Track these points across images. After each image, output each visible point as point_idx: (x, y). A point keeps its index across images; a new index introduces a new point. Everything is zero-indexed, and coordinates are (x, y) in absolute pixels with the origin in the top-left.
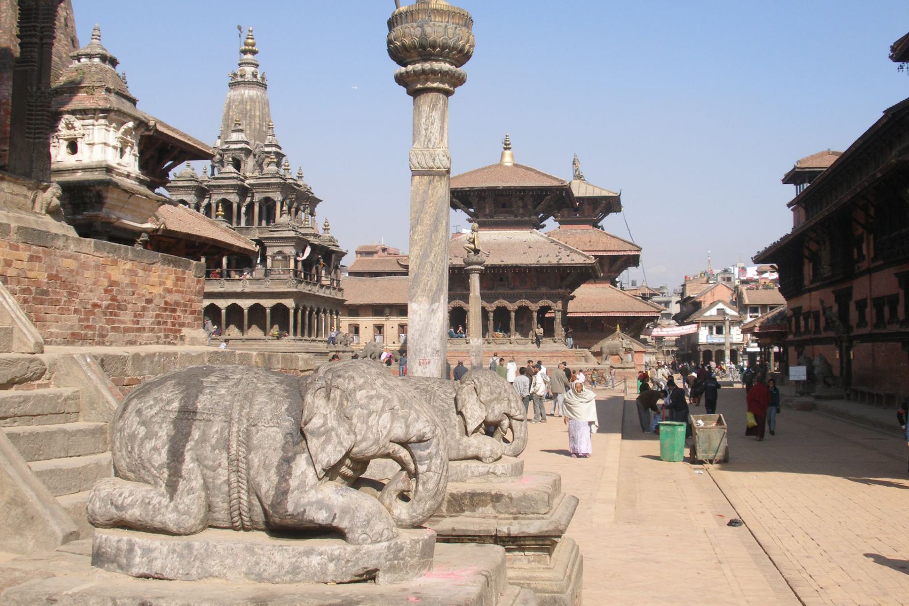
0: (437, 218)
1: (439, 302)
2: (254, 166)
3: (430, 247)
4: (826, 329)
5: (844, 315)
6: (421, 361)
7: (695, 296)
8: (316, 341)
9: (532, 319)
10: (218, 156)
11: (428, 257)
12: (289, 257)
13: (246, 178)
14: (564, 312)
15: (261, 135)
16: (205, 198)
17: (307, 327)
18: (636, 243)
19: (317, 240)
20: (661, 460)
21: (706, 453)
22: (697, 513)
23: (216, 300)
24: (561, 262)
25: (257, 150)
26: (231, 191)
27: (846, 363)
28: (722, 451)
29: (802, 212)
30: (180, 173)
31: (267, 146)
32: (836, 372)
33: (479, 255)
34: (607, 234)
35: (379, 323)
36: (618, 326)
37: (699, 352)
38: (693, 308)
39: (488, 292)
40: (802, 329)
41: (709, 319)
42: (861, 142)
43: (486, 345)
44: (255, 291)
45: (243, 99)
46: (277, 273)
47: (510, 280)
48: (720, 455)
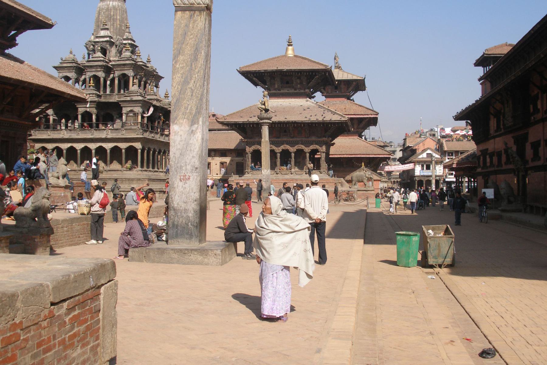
0: (196, 49)
1: (198, 124)
2: (116, 53)
3: (191, 75)
4: (506, 164)
5: (521, 152)
6: (182, 177)
8: (158, 171)
9: (306, 158)
10: (92, 47)
11: (188, 83)
12: (138, 114)
13: (110, 61)
14: (327, 154)
15: (121, 32)
16: (82, 75)
17: (151, 162)
18: (375, 110)
19: (159, 103)
20: (398, 266)
21: (436, 259)
22: (447, 344)
23: (89, 144)
24: (325, 119)
25: (118, 42)
26: (99, 70)
27: (523, 186)
28: (450, 257)
29: (488, 84)
30: (66, 58)
31: (125, 39)
32: (516, 192)
33: (268, 113)
34: (356, 104)
36: (363, 163)
37: (415, 181)
39: (276, 140)
40: (488, 164)
42: (539, 26)
43: (275, 175)
44: (114, 137)
45: (108, 7)
46: (130, 125)
48: (448, 261)
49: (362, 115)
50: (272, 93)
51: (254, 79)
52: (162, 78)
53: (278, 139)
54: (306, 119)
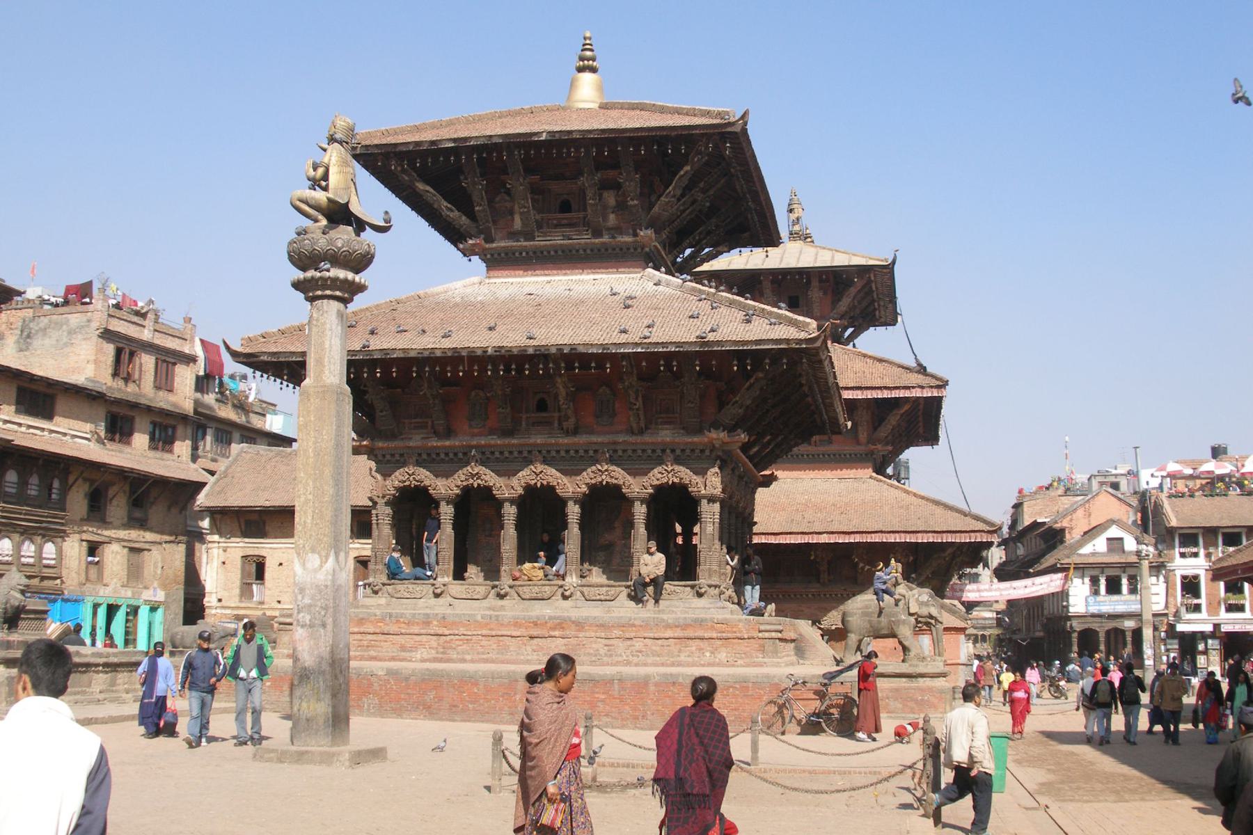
34: (865, 356)
37: (1070, 633)
38: (1043, 546)
41: (1091, 560)
43: (492, 601)
49: (886, 388)
50: (499, 251)
51: (421, 186)
53: (507, 441)
54: (623, 338)
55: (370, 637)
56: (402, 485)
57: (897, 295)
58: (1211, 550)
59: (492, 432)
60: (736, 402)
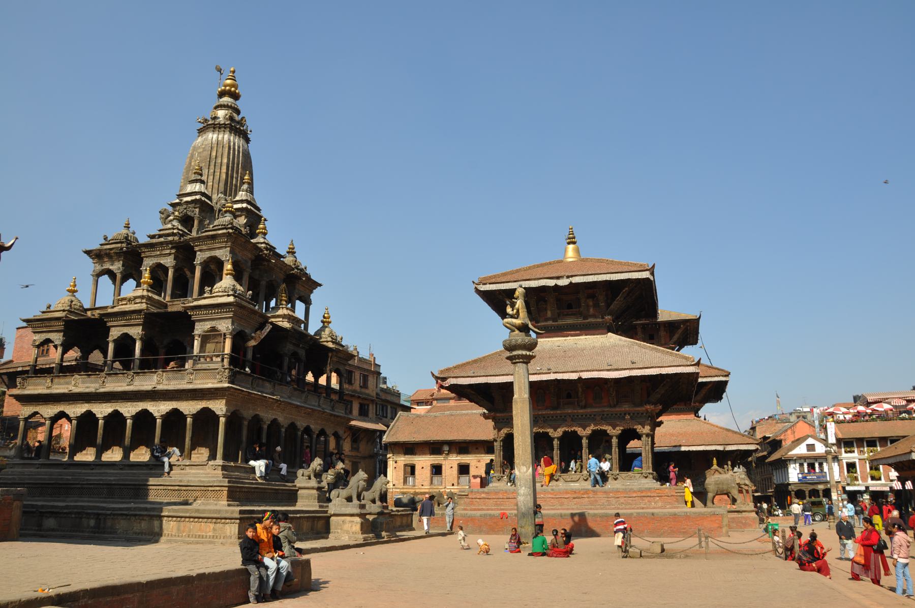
7: (771, 435)
12: (225, 335)
26: (168, 252)
35: (436, 462)
36: (715, 458)
39: (552, 412)
47: (580, 394)
52: (317, 285)
55: (500, 500)
56: (508, 432)
57: (700, 331)
58: (862, 449)
59: (547, 408)
60: (657, 392)
